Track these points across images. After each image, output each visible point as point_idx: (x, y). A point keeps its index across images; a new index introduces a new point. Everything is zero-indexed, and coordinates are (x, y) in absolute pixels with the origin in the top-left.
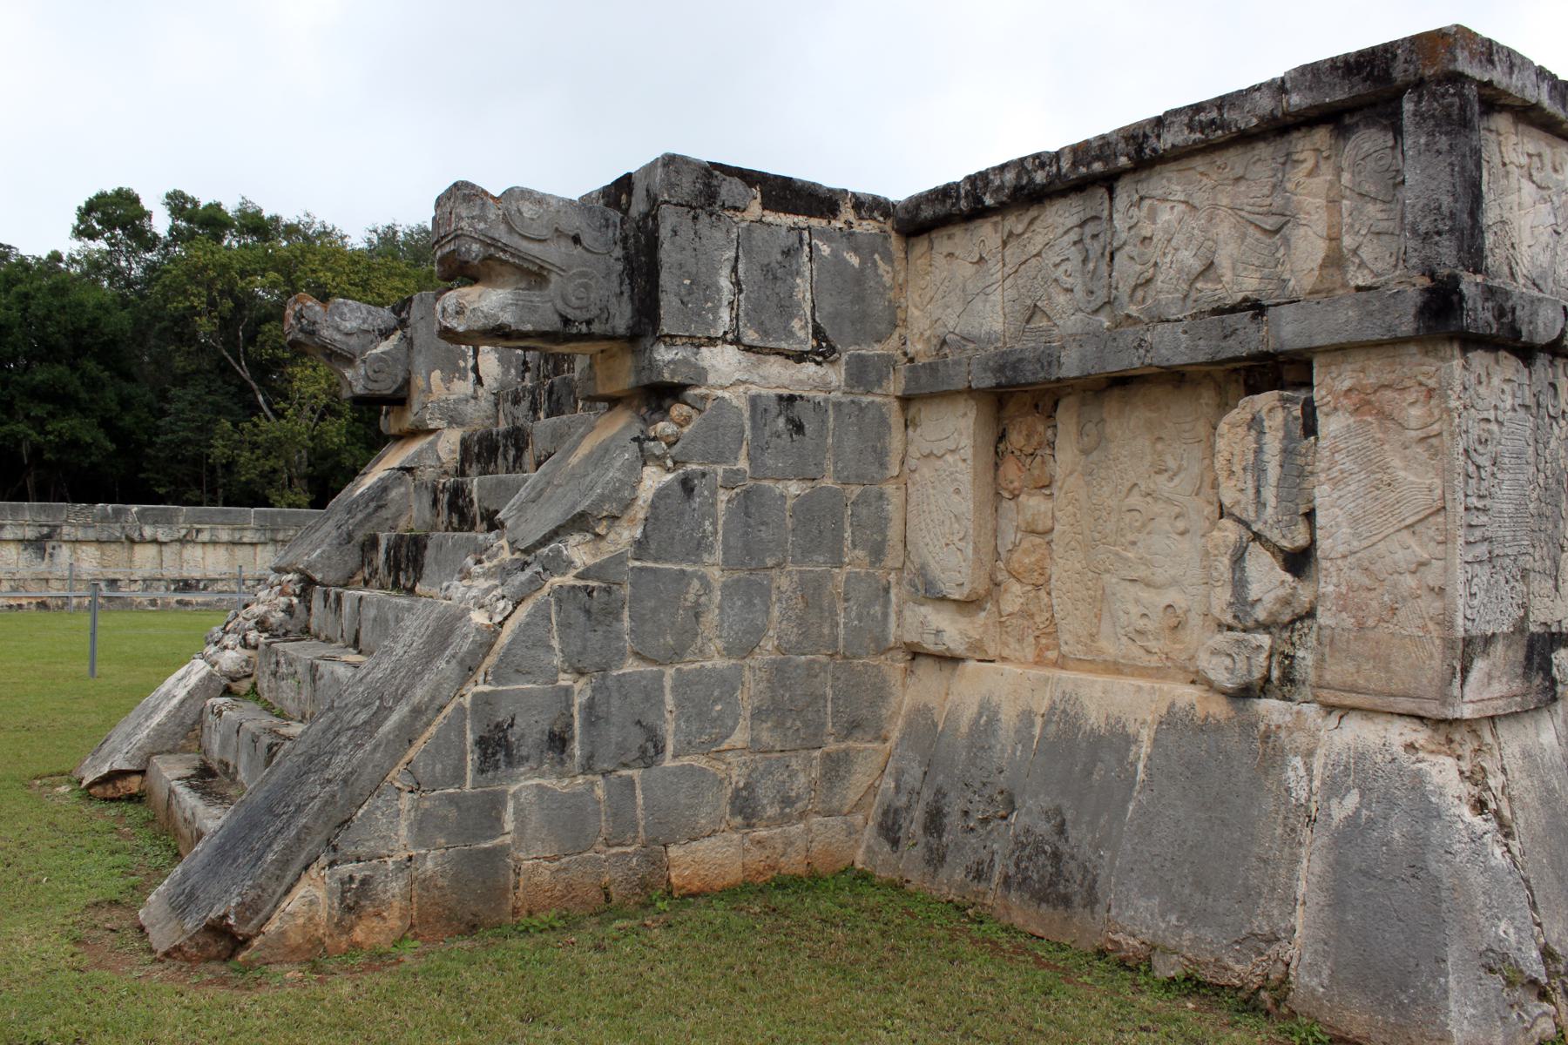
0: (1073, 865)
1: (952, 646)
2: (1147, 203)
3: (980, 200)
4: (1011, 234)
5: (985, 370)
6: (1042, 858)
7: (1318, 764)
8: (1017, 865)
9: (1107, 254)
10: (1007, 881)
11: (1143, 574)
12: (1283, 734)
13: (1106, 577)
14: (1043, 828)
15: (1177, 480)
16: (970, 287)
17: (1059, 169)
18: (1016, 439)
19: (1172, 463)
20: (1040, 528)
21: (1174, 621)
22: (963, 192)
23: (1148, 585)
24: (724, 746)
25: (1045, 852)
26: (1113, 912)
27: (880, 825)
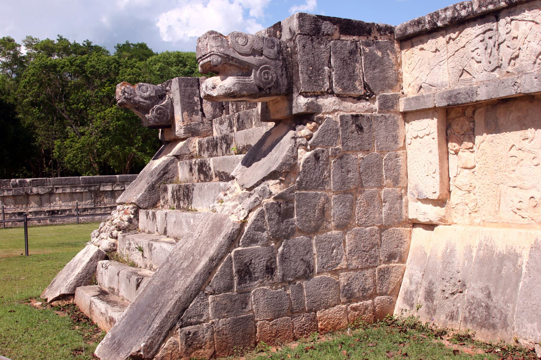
0: (495, 311)
1: (432, 220)
2: (513, 22)
3: (435, 24)
4: (450, 38)
5: (442, 99)
6: (481, 309)
8: (470, 312)
9: (496, 45)
10: (465, 319)
13: (501, 186)
14: (480, 296)
16: (432, 62)
17: (472, 9)
18: (456, 127)
20: (469, 166)
21: (534, 204)
22: (427, 21)
24: (338, 268)
25: (482, 306)
26: (516, 330)
27: (404, 299)
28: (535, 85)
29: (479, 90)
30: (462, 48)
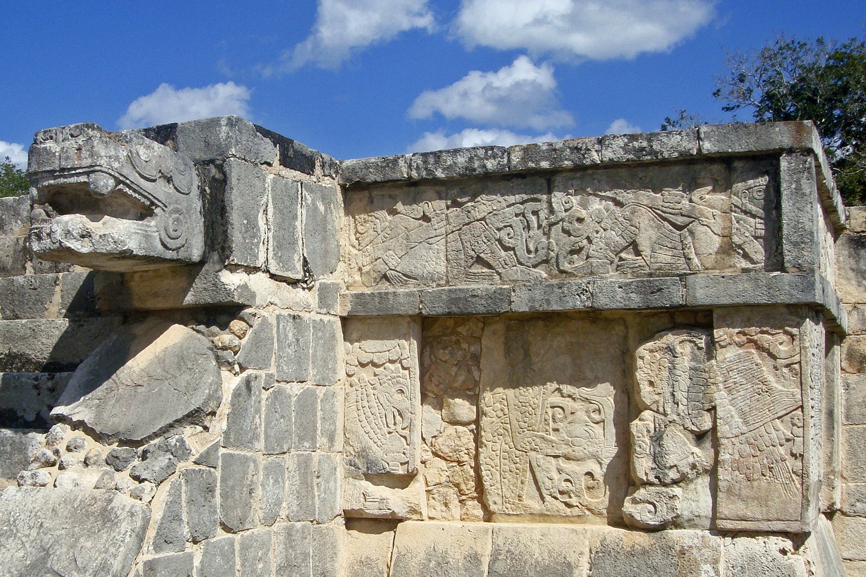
7: (721, 566)
11: (565, 451)
12: (694, 551)
23: (567, 458)
28: (618, 297)
30: (478, 220)
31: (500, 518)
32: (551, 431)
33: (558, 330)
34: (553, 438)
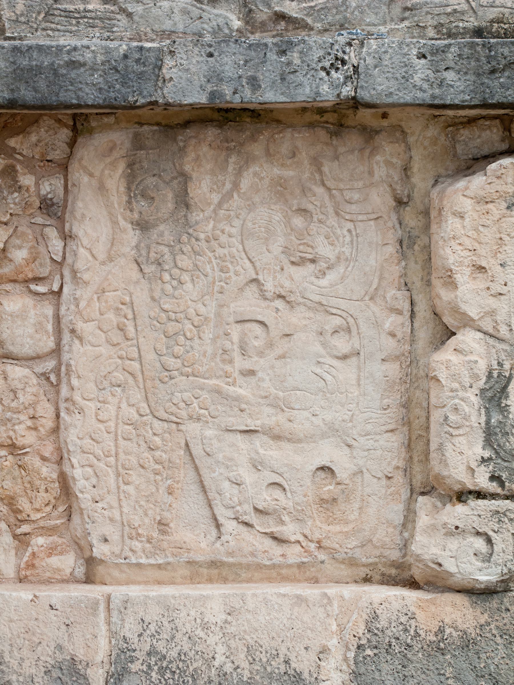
11: (270, 422)
13: (192, 428)
15: (331, 276)
19: (325, 250)
28: (417, 78)
29: (169, 62)
31: (116, 573)
32: (236, 374)
33: (257, 149)
34: (241, 392)
